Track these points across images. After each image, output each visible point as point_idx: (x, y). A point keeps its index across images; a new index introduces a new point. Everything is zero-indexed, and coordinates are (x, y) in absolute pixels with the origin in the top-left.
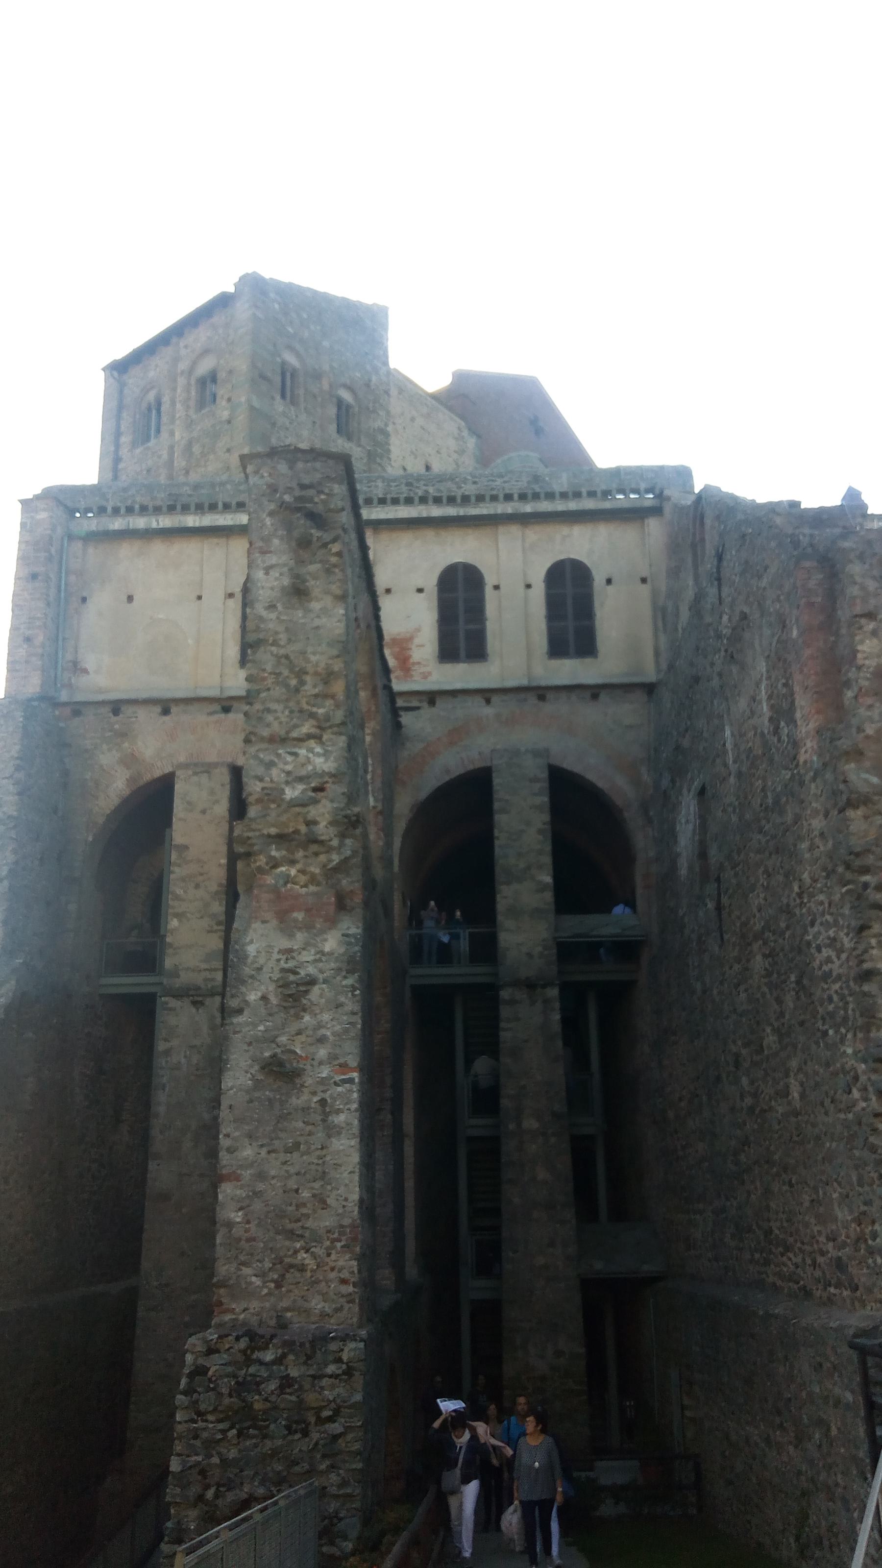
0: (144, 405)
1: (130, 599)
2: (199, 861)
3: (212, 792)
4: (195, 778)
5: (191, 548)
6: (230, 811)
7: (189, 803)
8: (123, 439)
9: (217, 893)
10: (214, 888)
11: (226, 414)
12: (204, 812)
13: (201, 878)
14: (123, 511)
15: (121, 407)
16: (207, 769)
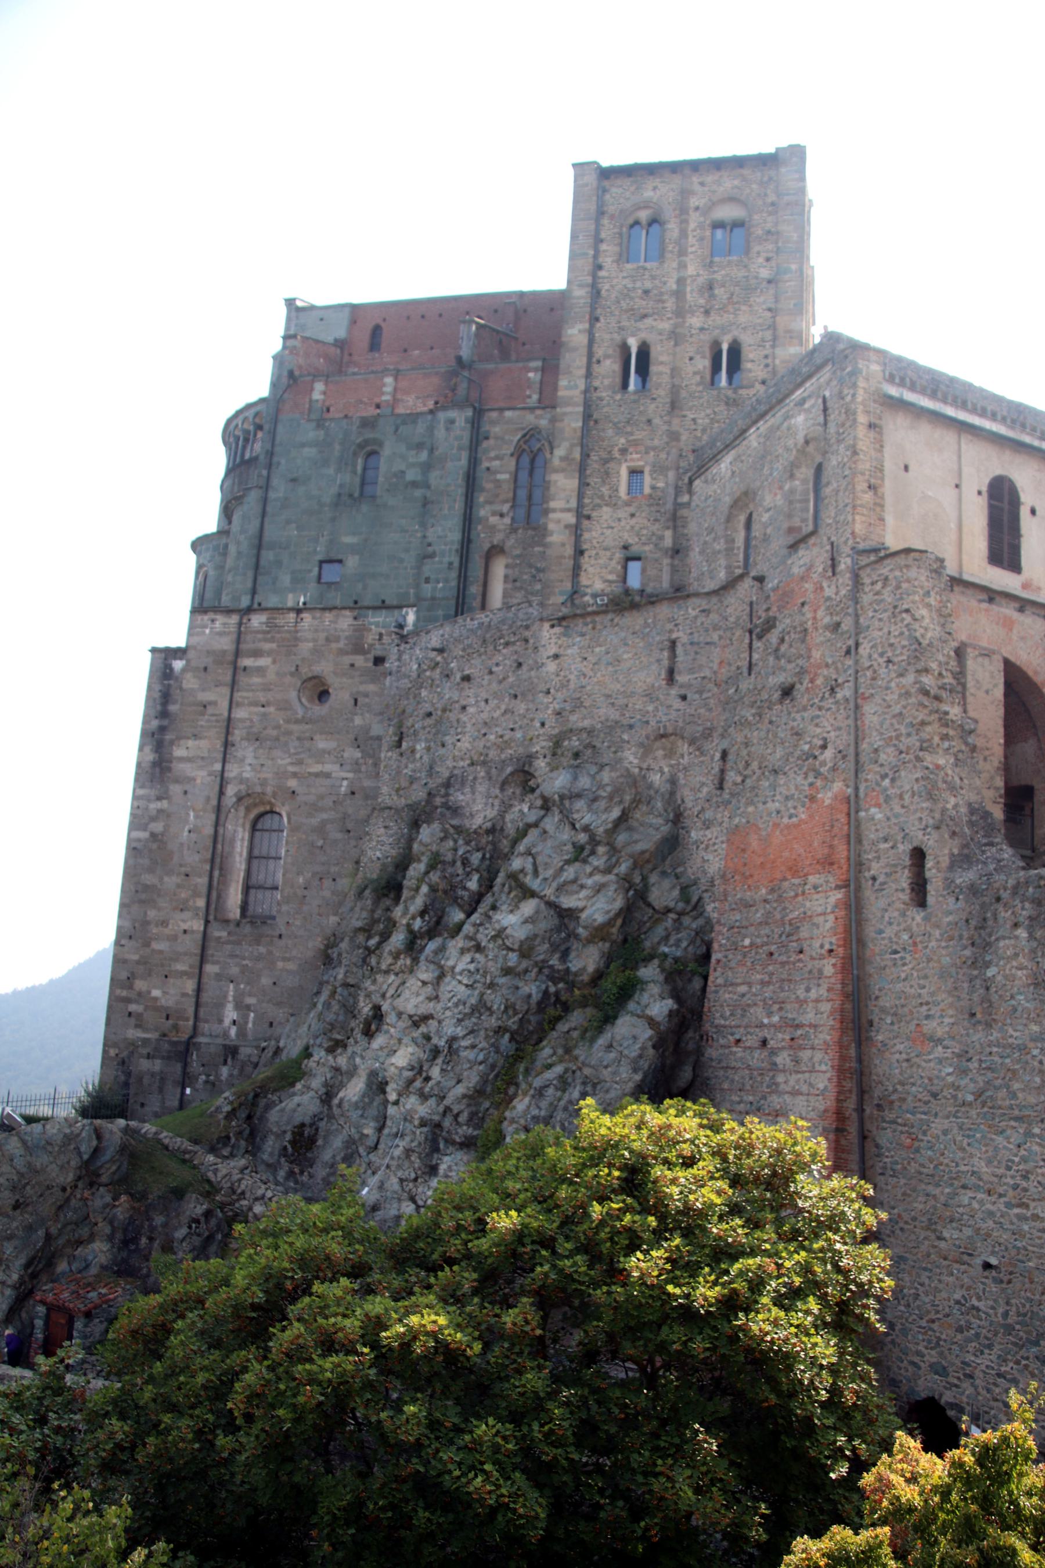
0: (631, 221)
1: (906, 468)
2: (985, 736)
3: (992, 677)
4: (980, 659)
5: (949, 437)
6: (1006, 695)
7: (978, 682)
8: (604, 247)
9: (998, 768)
10: (996, 764)
11: (765, 273)
12: (987, 692)
13: (987, 753)
14: (897, 380)
15: (601, 213)
16: (987, 654)
